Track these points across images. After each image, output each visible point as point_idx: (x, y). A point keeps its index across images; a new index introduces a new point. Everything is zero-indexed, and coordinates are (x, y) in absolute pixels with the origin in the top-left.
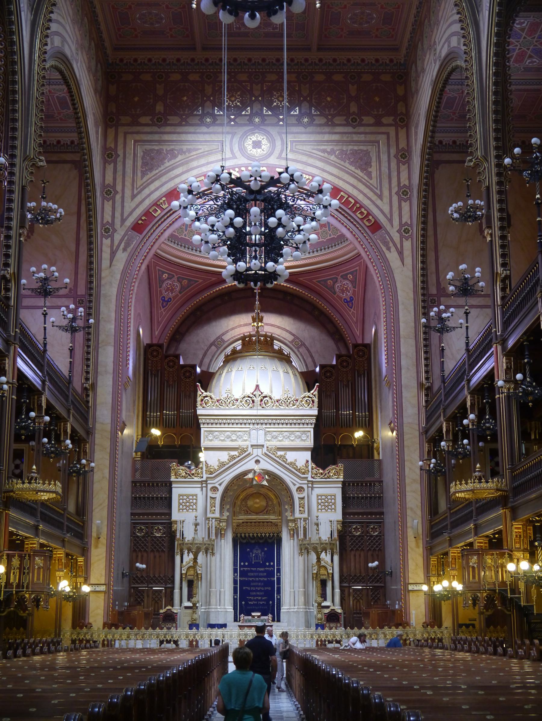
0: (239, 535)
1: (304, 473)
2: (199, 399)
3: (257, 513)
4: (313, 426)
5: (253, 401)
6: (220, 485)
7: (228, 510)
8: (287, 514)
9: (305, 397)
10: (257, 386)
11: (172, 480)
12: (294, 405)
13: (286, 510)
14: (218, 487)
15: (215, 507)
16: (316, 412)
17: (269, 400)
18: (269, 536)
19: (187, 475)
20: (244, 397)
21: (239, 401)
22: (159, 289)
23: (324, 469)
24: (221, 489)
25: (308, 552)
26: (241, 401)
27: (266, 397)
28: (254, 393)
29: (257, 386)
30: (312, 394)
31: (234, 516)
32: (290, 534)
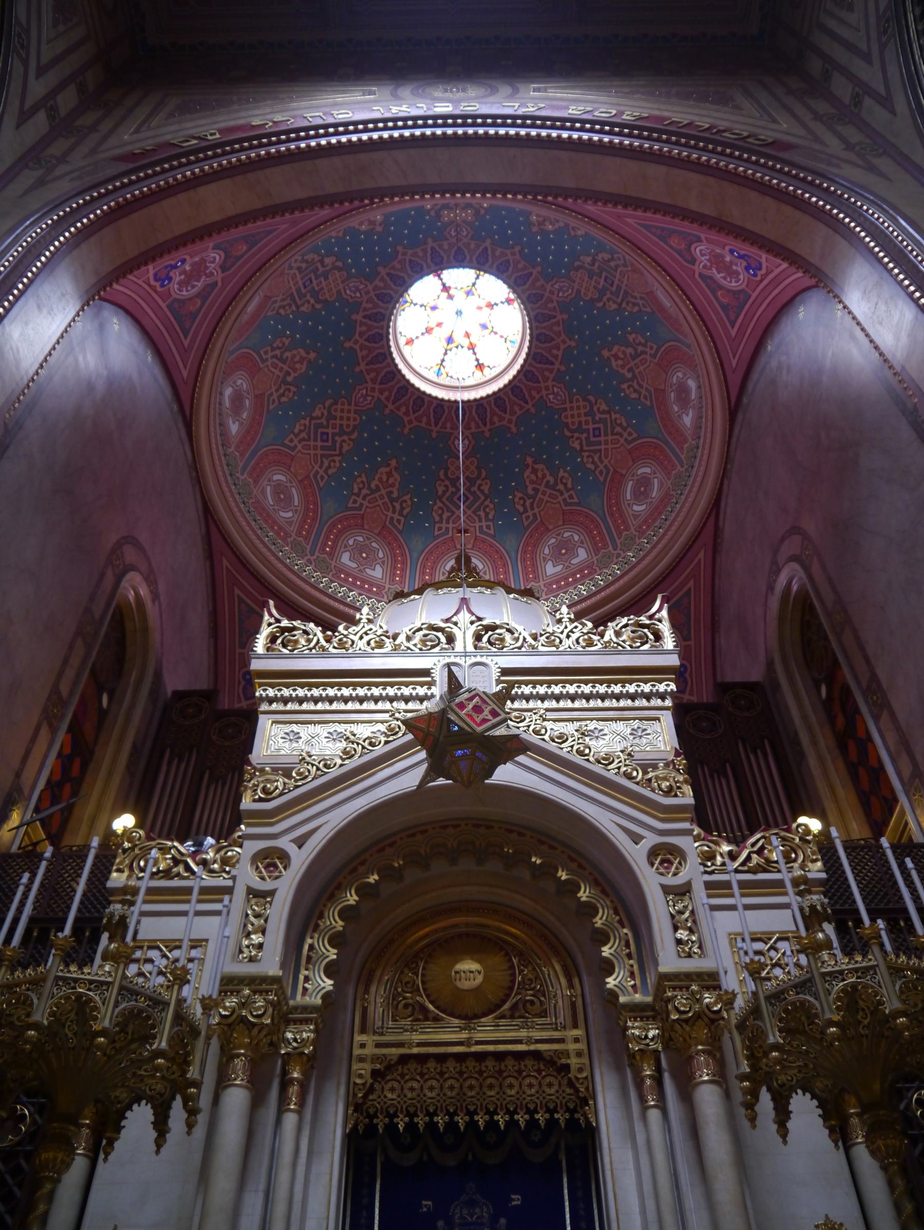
0: (381, 1123)
1: (669, 792)
2: (265, 632)
3: (470, 1018)
4: (668, 703)
5: (451, 639)
6: (300, 842)
7: (331, 970)
8: (611, 982)
9: (626, 626)
10: (464, 601)
11: (109, 884)
12: (590, 643)
13: (608, 968)
14: (292, 849)
15: (263, 932)
16: (674, 660)
17: (508, 637)
18: (532, 1123)
19: (181, 868)
20: (420, 629)
21: (401, 639)
22: (238, 651)
23: (738, 841)
24: (301, 859)
25: (783, 1115)
26: (409, 639)
27: (492, 628)
28: (454, 619)
29: (464, 601)
30: (651, 617)
31: (363, 1031)
32: (639, 1083)
